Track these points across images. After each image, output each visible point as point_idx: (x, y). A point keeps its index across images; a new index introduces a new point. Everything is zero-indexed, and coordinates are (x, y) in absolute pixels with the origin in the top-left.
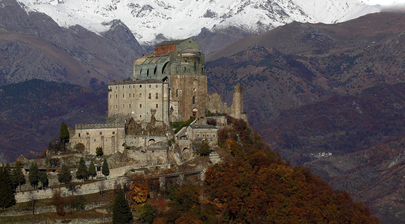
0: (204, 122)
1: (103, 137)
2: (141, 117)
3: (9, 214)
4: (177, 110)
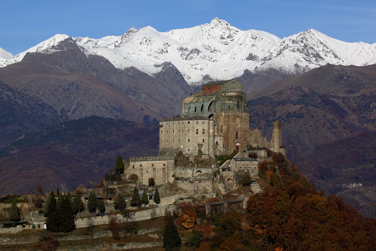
0: (246, 156)
1: (154, 169)
2: (189, 150)
3: (71, 238)
4: (222, 144)
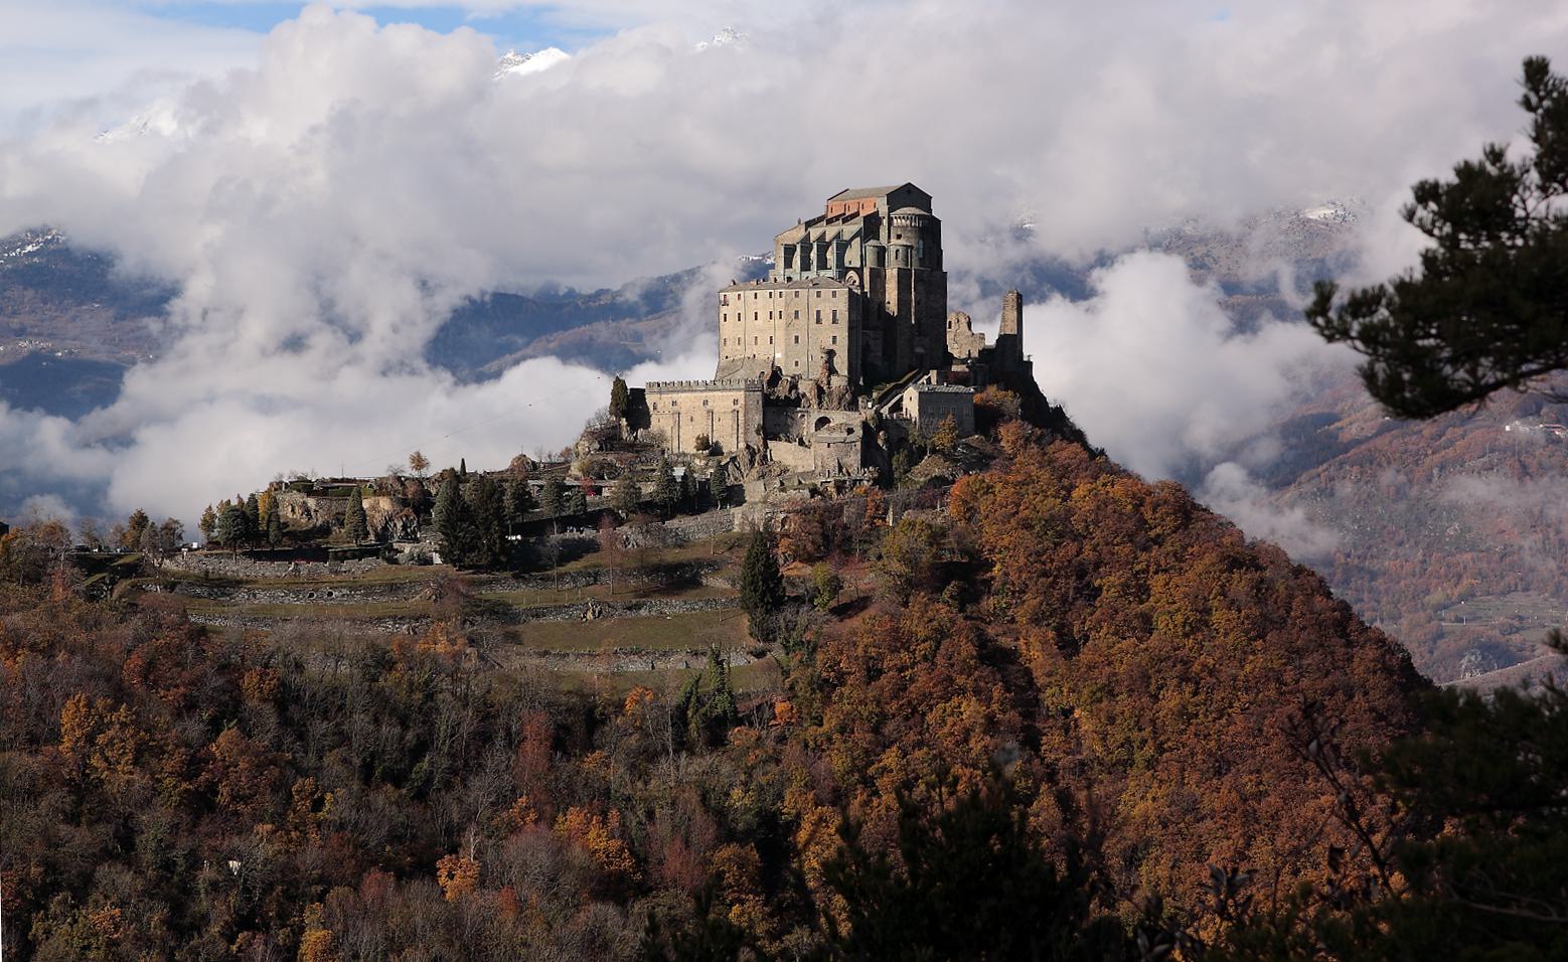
2: (797, 363)
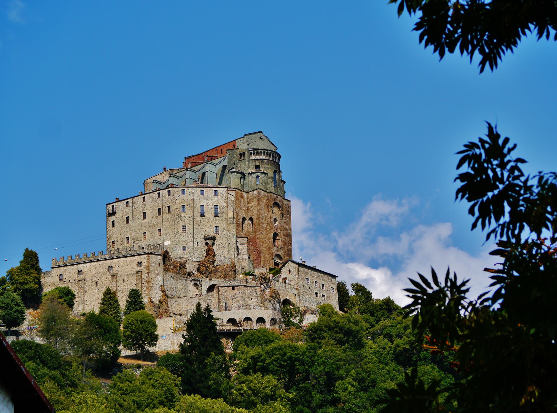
2: (184, 248)
